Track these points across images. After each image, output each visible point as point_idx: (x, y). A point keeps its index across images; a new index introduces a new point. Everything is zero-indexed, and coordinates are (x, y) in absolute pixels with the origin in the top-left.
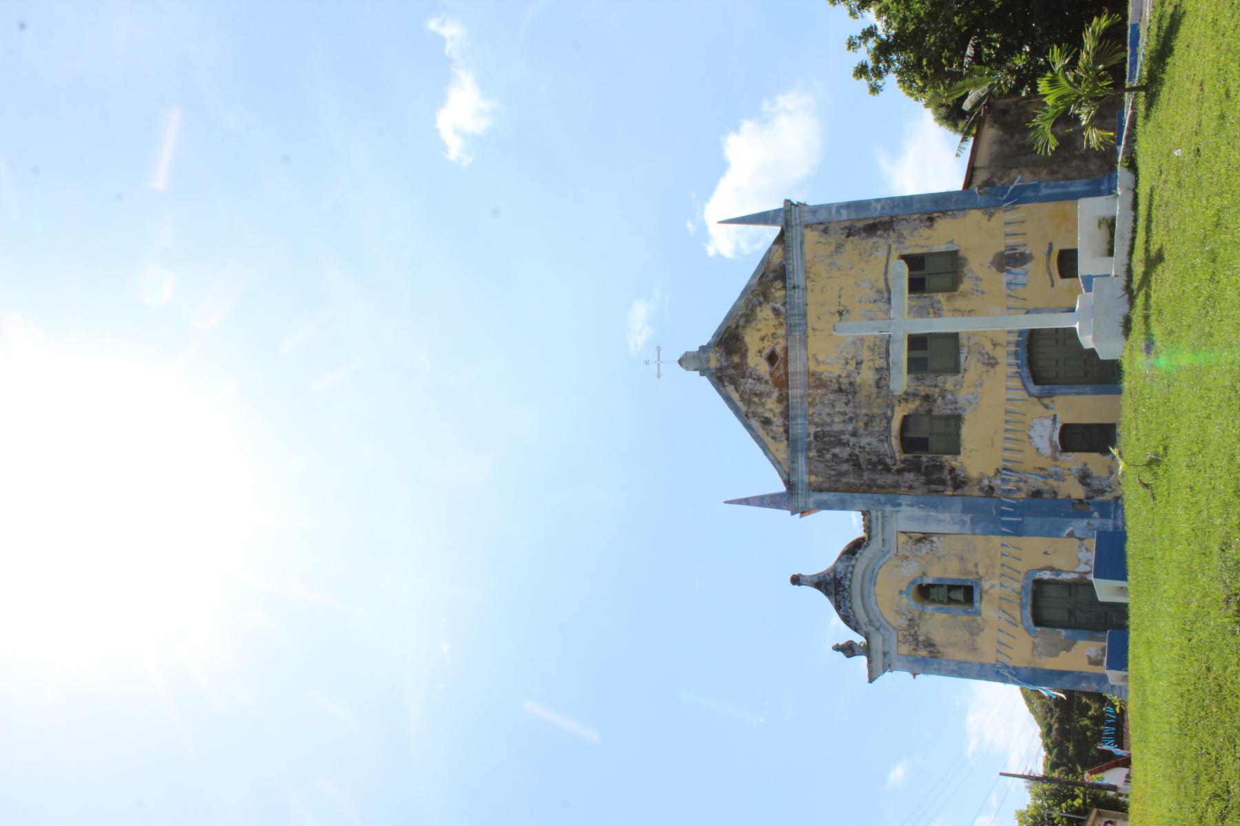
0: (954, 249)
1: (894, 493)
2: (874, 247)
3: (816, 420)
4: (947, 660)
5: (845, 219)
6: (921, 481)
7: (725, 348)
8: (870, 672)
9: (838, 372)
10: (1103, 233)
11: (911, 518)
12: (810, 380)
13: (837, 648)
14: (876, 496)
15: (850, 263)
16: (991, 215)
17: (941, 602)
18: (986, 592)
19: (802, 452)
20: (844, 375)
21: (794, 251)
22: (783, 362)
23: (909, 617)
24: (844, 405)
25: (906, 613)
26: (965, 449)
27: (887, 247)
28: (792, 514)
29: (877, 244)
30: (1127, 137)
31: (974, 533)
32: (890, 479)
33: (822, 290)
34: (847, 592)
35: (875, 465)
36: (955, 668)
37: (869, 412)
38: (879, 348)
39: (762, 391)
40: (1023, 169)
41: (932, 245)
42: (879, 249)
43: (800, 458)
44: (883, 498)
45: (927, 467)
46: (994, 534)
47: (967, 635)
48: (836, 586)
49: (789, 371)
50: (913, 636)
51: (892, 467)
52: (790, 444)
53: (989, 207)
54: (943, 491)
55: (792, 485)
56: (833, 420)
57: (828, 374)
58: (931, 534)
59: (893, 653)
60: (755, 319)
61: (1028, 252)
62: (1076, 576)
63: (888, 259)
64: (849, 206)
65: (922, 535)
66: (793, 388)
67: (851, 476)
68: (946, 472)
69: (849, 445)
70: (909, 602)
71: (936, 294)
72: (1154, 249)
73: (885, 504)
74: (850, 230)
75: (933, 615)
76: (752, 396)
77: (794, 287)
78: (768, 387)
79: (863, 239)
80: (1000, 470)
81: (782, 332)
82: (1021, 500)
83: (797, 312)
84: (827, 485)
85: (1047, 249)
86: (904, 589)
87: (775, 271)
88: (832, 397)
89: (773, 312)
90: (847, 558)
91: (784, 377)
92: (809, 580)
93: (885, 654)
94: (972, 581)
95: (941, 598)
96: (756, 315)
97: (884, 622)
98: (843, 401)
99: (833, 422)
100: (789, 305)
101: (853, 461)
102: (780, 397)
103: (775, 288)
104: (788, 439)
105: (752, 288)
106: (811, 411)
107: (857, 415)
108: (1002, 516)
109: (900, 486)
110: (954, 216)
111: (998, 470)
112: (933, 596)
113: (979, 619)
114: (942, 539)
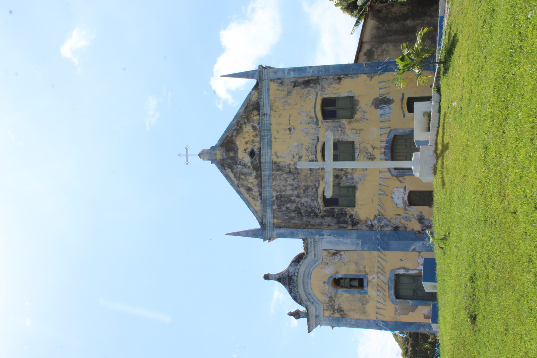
0: (352, 95)
1: (320, 228)
2: (309, 93)
3: (277, 188)
4: (350, 319)
5: (292, 77)
6: (335, 222)
7: (226, 148)
8: (309, 327)
9: (288, 162)
10: (425, 120)
11: (330, 242)
12: (273, 166)
13: (290, 314)
14: (310, 231)
15: (295, 102)
16: (372, 78)
17: (346, 287)
18: (370, 281)
19: (269, 206)
20: (292, 164)
21: (264, 94)
22: (258, 156)
23: (329, 296)
24: (292, 180)
25: (328, 294)
26: (358, 204)
27: (315, 94)
28: (264, 241)
29: (310, 92)
30: (437, 78)
31: (363, 250)
32: (318, 221)
33: (280, 116)
34: (295, 283)
35: (309, 213)
36: (354, 323)
37: (306, 184)
38: (311, 149)
39: (247, 172)
40: (389, 44)
41: (340, 93)
42: (311, 94)
43: (268, 210)
44: (314, 231)
45: (337, 214)
46: (374, 250)
47: (361, 305)
48: (289, 280)
49: (262, 161)
50: (331, 306)
51: (319, 214)
52: (263, 202)
53: (371, 73)
54: (346, 227)
55: (264, 225)
56: (286, 188)
57: (283, 163)
58: (340, 251)
59: (321, 316)
60: (242, 132)
61: (391, 98)
62: (417, 272)
63: (316, 100)
64: (295, 70)
65: (336, 251)
66: (263, 171)
67: (297, 219)
68: (348, 217)
69: (295, 202)
70: (329, 288)
71: (341, 120)
72: (446, 142)
73: (315, 235)
74: (295, 83)
75: (342, 294)
76: (241, 175)
77: (264, 114)
78: (250, 170)
79: (302, 88)
80: (377, 216)
81: (257, 139)
82: (388, 232)
83: (266, 128)
84: (283, 224)
85: (401, 97)
86: (326, 281)
87: (253, 105)
88: (285, 176)
89: (252, 128)
90: (295, 264)
91: (259, 164)
92: (274, 277)
93: (316, 317)
94: (362, 276)
95: (346, 285)
96: (243, 130)
97: (316, 300)
98: (292, 178)
99: (286, 190)
100: (262, 124)
101: (297, 211)
102: (257, 176)
103: (254, 115)
104: (261, 199)
105: (240, 114)
106: (274, 183)
107: (299, 186)
109: (323, 225)
110: (352, 78)
111: (375, 216)
112: (342, 284)
113: (367, 296)
114: (346, 253)
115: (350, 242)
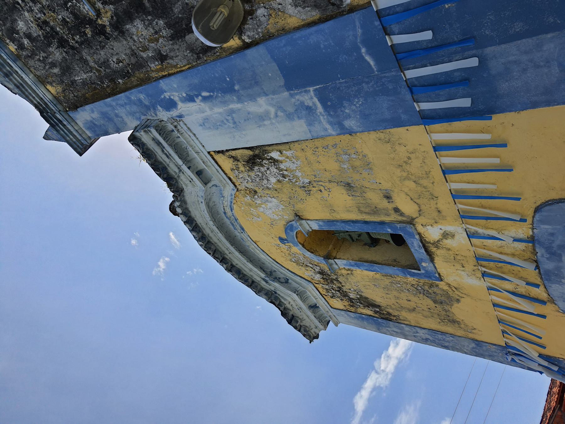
46: (397, 123)
65: (250, 153)
108: (402, 69)
114: (289, 153)
115: (272, 110)
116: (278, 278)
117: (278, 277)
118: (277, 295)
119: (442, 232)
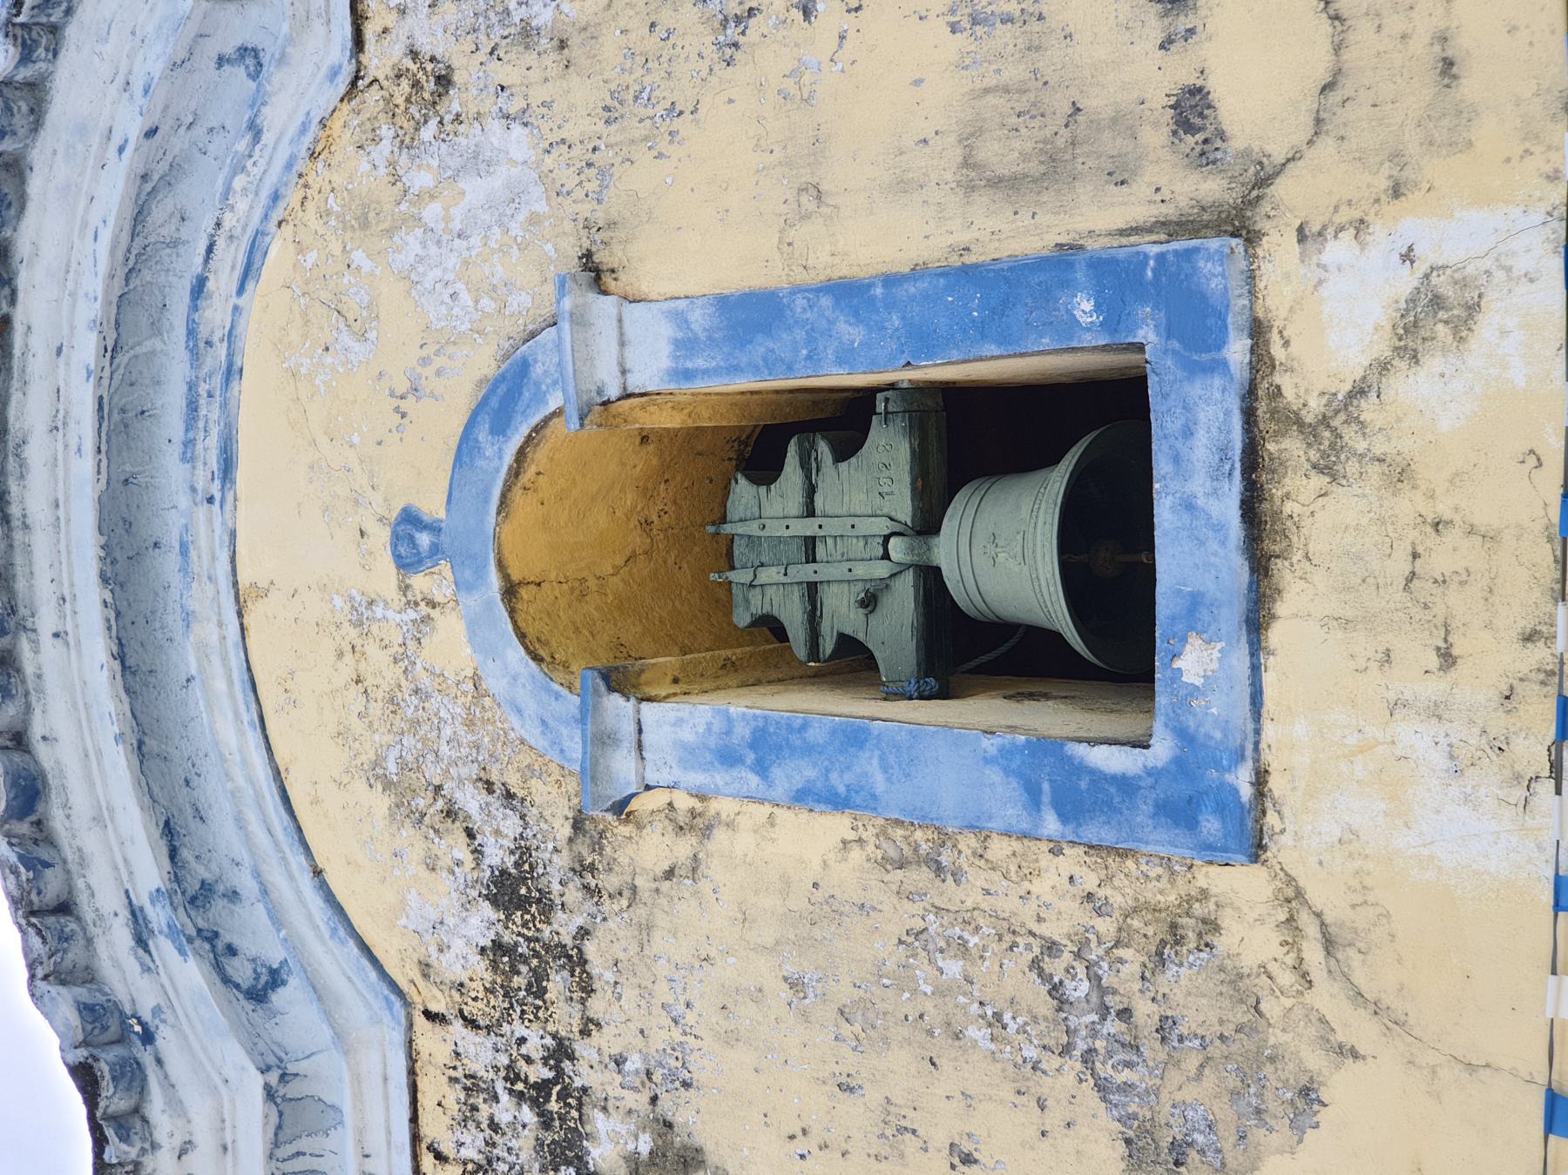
25: (471, 801)
75: (697, 825)
95: (841, 613)
116: (220, 945)
117: (226, 937)
118: (146, 1058)
119: (1405, 281)
